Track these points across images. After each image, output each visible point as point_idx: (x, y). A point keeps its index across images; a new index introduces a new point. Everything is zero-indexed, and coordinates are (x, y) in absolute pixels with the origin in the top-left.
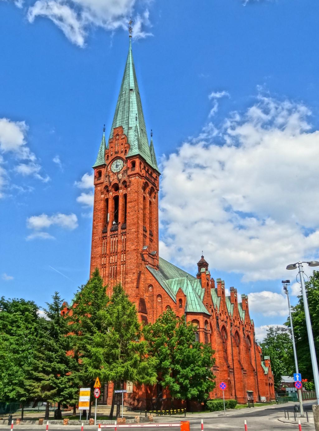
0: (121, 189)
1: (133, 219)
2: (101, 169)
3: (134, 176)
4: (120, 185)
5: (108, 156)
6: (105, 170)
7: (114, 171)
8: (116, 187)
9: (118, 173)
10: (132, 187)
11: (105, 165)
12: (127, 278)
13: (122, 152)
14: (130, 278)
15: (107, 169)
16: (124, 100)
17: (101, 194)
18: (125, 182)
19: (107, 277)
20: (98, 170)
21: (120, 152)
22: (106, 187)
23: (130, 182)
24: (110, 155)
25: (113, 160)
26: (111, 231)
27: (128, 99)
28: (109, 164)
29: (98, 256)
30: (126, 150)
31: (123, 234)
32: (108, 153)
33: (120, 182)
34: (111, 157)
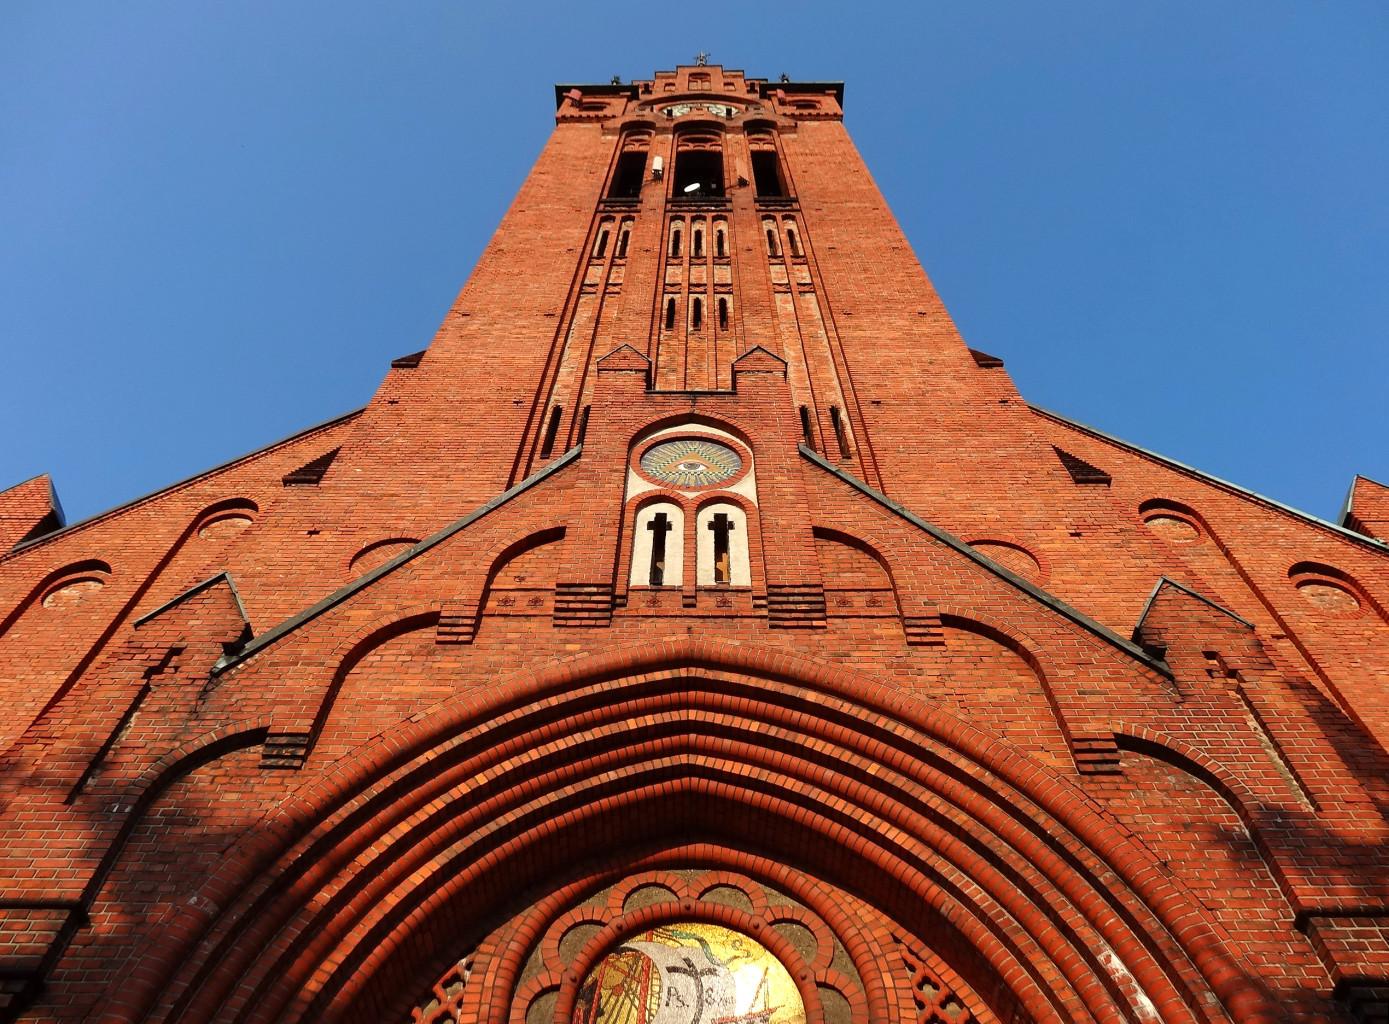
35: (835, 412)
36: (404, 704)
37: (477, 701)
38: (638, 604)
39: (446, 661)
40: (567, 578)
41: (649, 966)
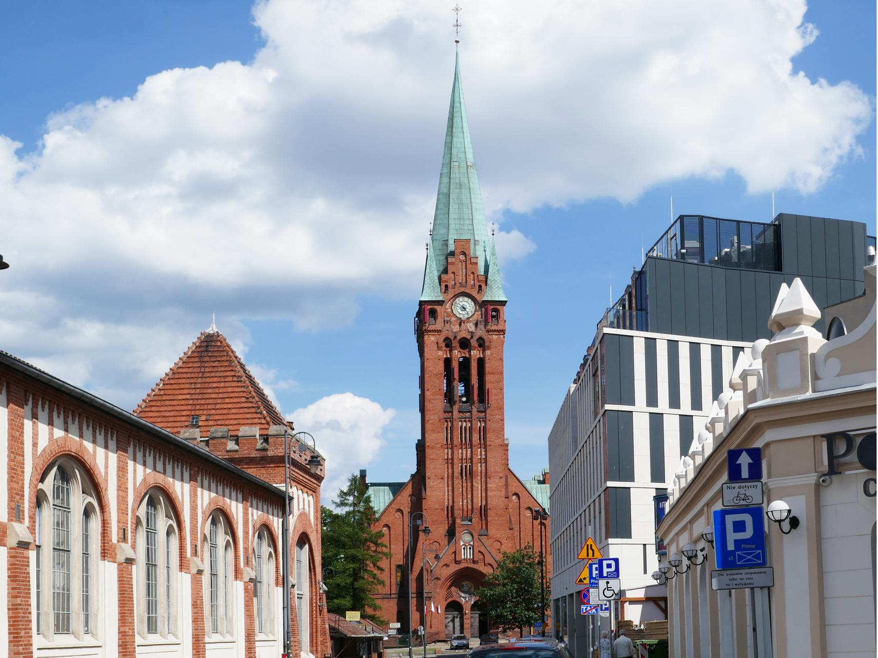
4: (474, 342)
5: (446, 286)
8: (465, 344)
21: (469, 286)
24: (450, 285)
30: (480, 286)
33: (472, 337)
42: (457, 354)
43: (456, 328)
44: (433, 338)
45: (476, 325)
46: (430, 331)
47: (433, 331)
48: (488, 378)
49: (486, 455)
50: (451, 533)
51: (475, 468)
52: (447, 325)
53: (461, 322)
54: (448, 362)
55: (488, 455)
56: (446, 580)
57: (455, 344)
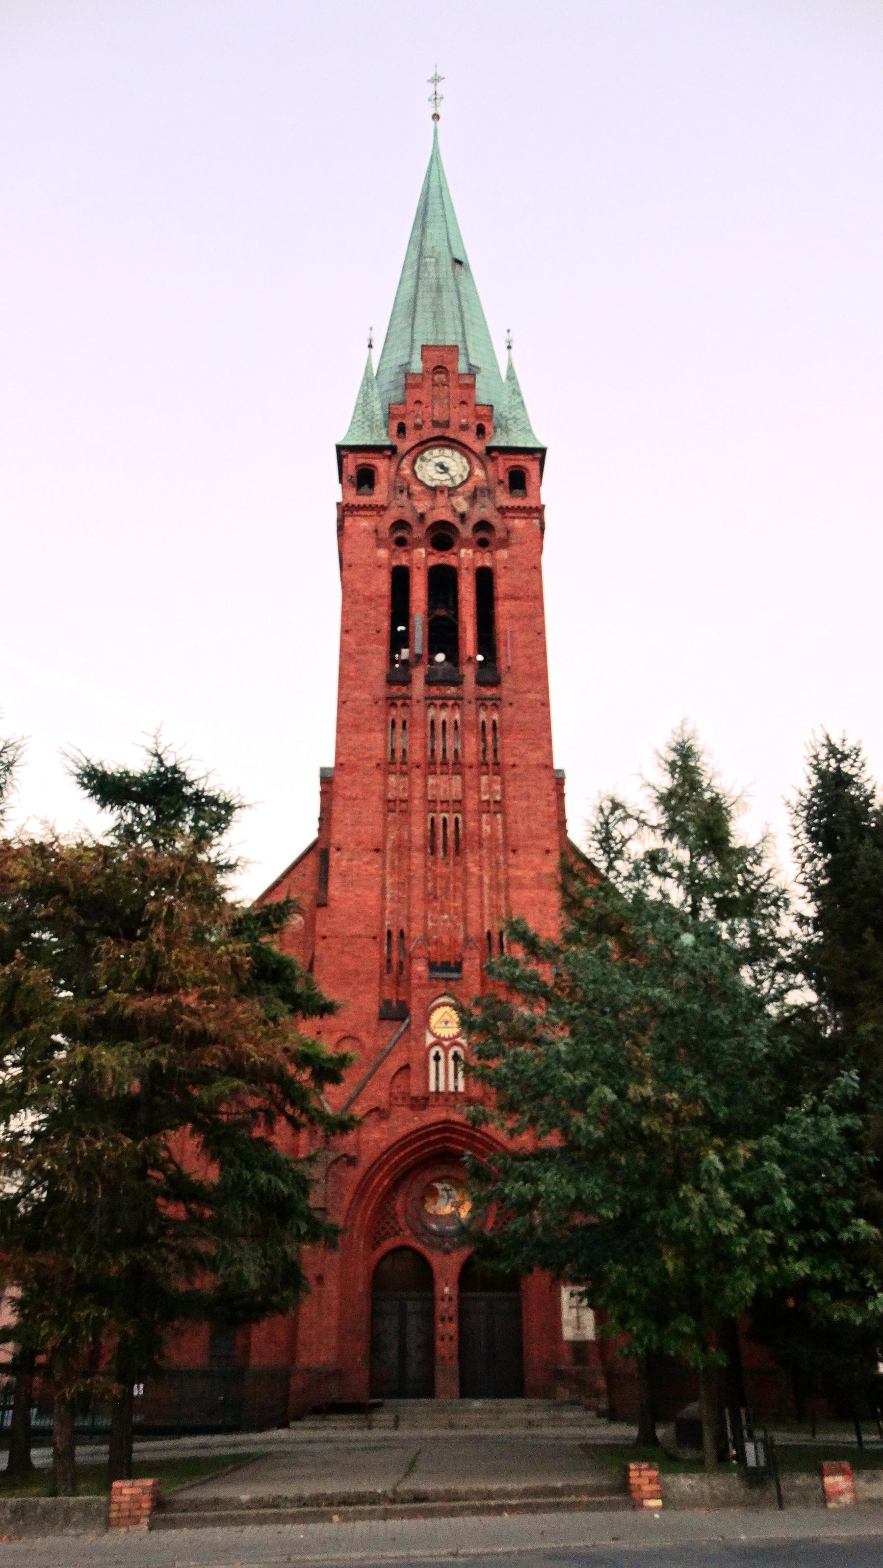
0: (468, 547)
1: (529, 657)
2: (373, 462)
3: (526, 515)
4: (466, 531)
6: (393, 470)
7: (429, 483)
8: (442, 536)
9: (452, 491)
10: (516, 549)
11: (393, 449)
12: (517, 867)
13: (464, 428)
14: (534, 868)
15: (398, 469)
16: (433, 282)
17: (379, 546)
18: (483, 525)
19: (418, 850)
20: (361, 461)
22: (400, 524)
23: (508, 532)
24: (409, 423)
25: (424, 445)
26: (429, 682)
27: (451, 282)
28: (409, 451)
29: (374, 763)
31: (482, 702)
32: (403, 416)
34: (419, 432)
35: (501, 934)
36: (375, 1141)
37: (394, 1139)
38: (432, 1100)
39: (384, 1125)
40: (412, 1094)
41: (436, 1190)
42: (421, 558)
43: (422, 506)
44: (364, 524)
45: (473, 498)
46: (359, 508)
47: (365, 508)
48: (503, 608)
49: (503, 790)
50: (395, 1013)
51: (472, 825)
52: (404, 497)
53: (434, 491)
54: (400, 578)
55: (511, 790)
56: (378, 1164)
57: (419, 532)
